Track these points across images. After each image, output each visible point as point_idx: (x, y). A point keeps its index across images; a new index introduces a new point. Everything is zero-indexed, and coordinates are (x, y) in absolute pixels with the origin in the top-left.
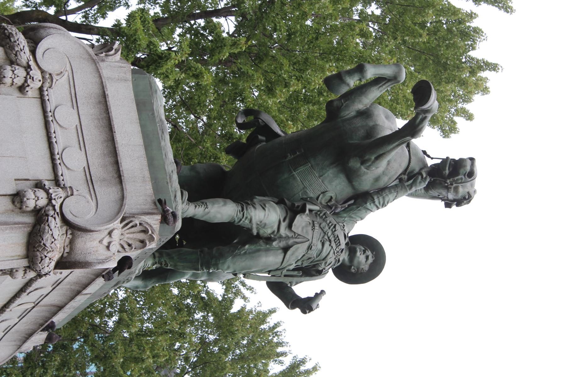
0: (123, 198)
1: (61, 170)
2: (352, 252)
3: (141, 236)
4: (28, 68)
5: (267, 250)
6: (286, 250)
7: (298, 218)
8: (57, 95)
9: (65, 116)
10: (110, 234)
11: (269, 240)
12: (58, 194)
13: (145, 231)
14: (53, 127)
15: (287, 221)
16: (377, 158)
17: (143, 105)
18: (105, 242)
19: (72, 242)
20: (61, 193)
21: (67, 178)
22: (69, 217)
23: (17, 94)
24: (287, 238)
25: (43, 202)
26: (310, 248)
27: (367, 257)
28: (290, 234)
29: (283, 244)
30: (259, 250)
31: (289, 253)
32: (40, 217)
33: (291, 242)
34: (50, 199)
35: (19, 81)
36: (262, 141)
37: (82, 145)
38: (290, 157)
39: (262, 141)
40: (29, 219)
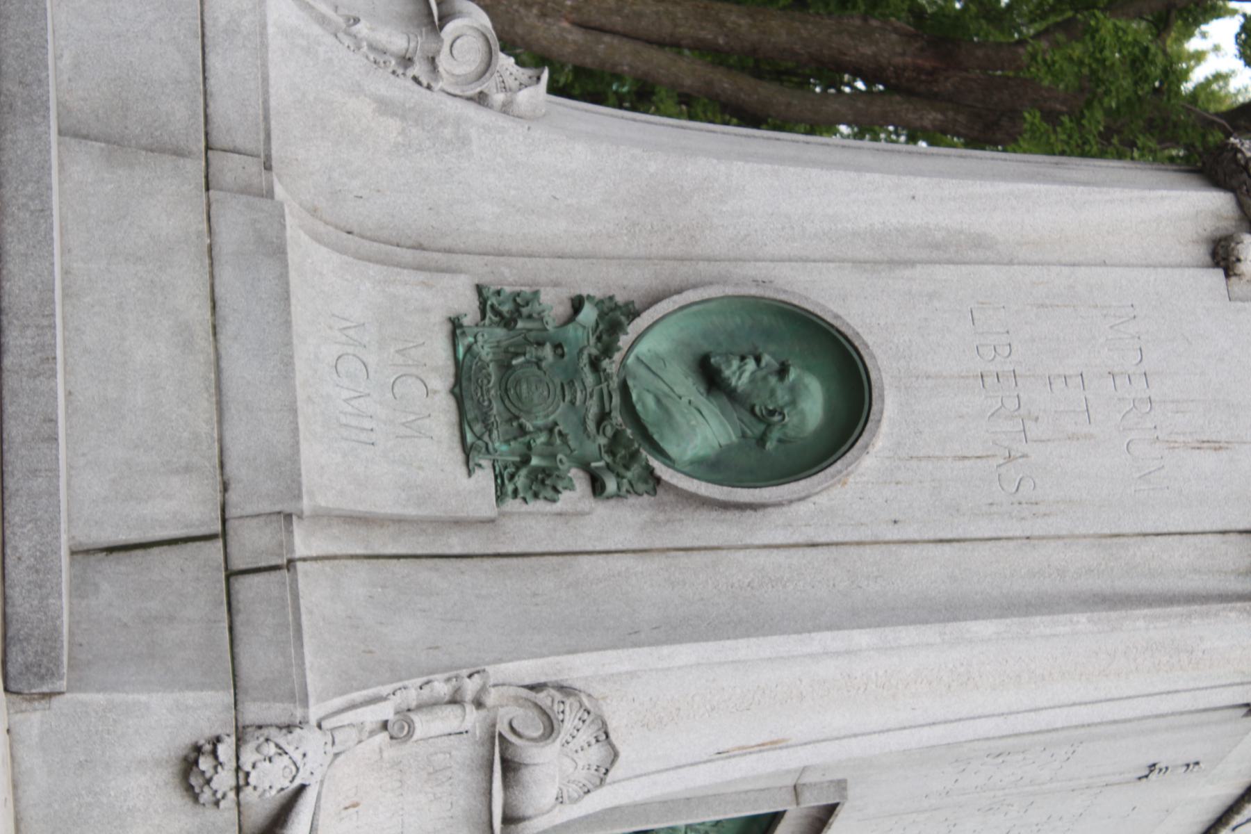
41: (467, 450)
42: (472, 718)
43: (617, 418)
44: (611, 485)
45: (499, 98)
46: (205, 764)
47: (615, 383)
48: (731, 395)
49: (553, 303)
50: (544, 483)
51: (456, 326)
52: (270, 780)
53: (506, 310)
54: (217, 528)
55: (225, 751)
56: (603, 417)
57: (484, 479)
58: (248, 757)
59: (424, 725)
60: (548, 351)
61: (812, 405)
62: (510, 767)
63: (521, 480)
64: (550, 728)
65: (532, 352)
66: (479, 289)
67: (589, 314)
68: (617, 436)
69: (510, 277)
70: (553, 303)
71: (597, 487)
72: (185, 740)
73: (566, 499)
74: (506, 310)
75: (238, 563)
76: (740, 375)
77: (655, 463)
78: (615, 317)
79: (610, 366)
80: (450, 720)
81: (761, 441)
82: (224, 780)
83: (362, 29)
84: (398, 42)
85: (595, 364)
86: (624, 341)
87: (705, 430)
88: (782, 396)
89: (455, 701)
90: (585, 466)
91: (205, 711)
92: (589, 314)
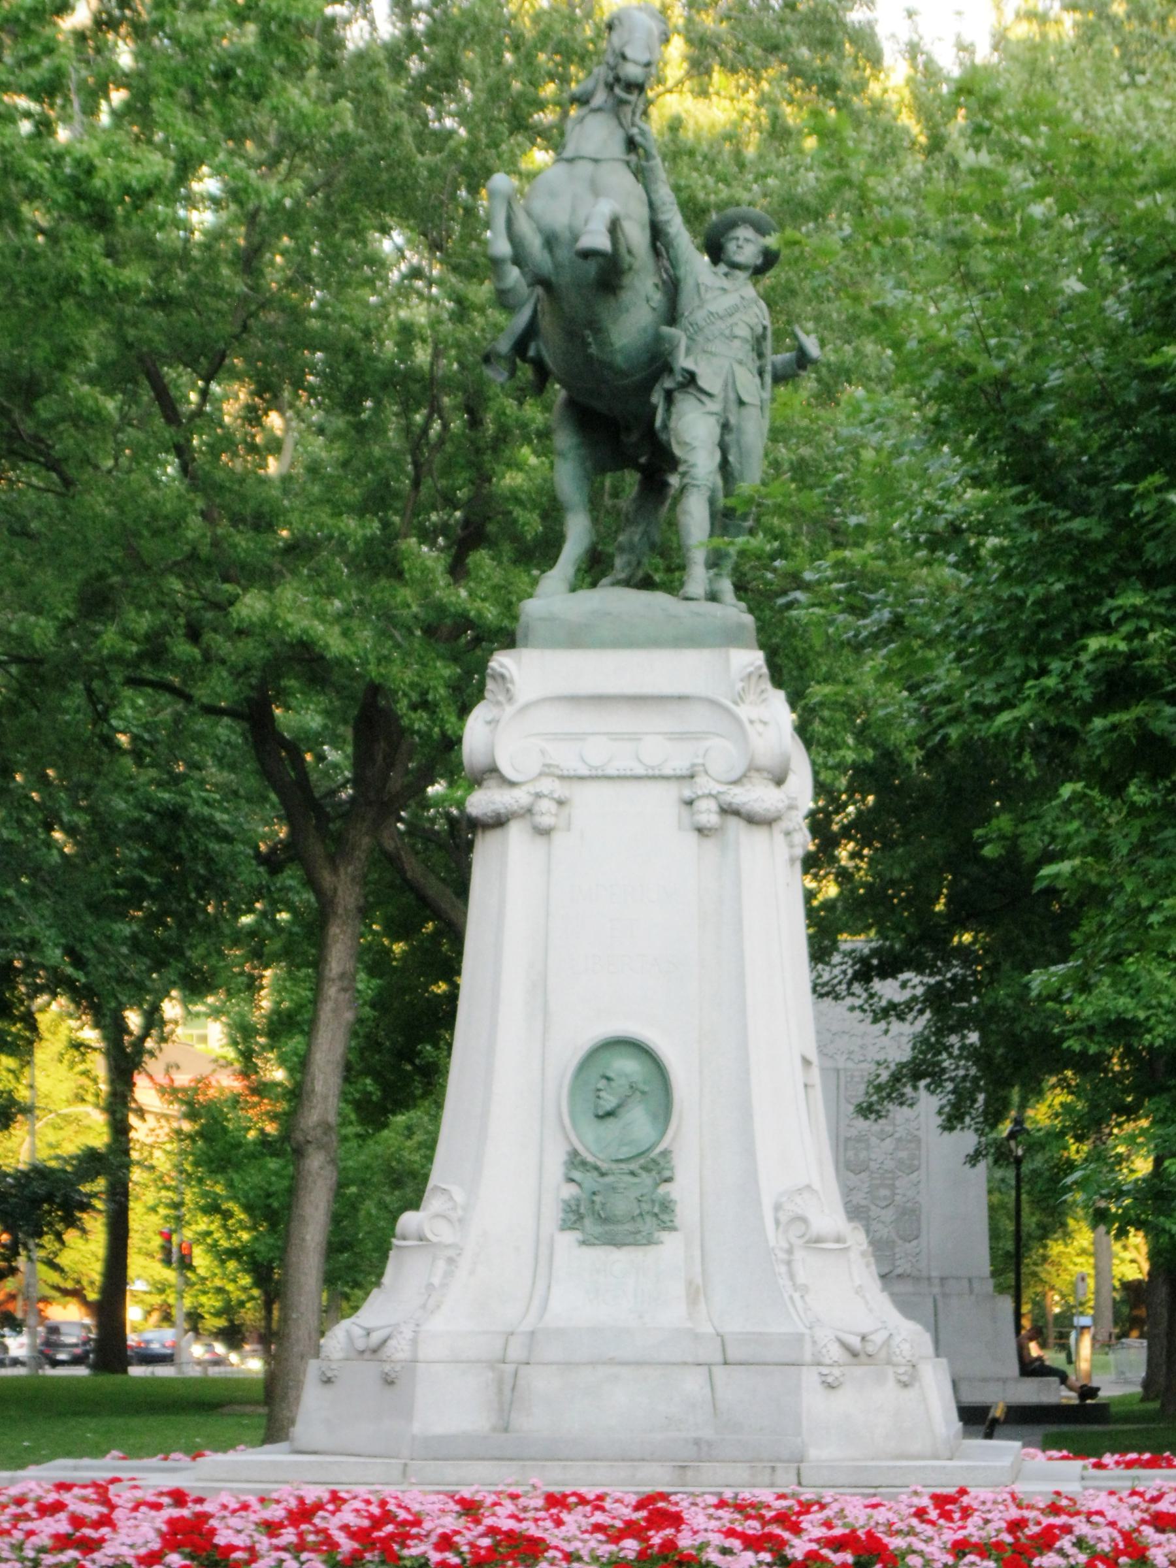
0: (713, 702)
1: (667, 771)
2: (735, 266)
3: (754, 679)
4: (539, 796)
5: (739, 429)
6: (741, 403)
7: (702, 383)
8: (567, 758)
9: (599, 753)
10: (751, 722)
11: (725, 427)
12: (704, 784)
13: (750, 675)
14: (611, 771)
15: (704, 398)
16: (630, 252)
17: (576, 637)
18: (760, 727)
19: (758, 770)
20: (701, 780)
21: (679, 765)
22: (735, 775)
23: (566, 810)
24: (726, 400)
25: (712, 805)
26: (740, 362)
27: (747, 240)
28: (720, 397)
29: (733, 406)
30: (738, 442)
31: (745, 398)
32: (728, 811)
33: (732, 396)
34: (710, 795)
35: (553, 807)
36: (538, 351)
37: (635, 737)
38: (593, 350)
39: (538, 351)
40: (733, 823)
41: (650, 1243)
42: (799, 1255)
43: (633, 1166)
44: (667, 1174)
45: (460, 1212)
46: (830, 1379)
47: (614, 1166)
48: (620, 1106)
49: (569, 1191)
50: (666, 1206)
51: (584, 1243)
52: (835, 1352)
53: (574, 1216)
54: (704, 1369)
55: (825, 1370)
56: (633, 1173)
57: (665, 1236)
58: (827, 1361)
59: (801, 1279)
60: (597, 1198)
61: (627, 1066)
62: (818, 1240)
63: (665, 1217)
64: (803, 1220)
65: (598, 1207)
66: (562, 1229)
67: (577, 1175)
68: (643, 1168)
69: (552, 1214)
70: (569, 1191)
71: (668, 1180)
72: (820, 1388)
73: (675, 1196)
74: (574, 1216)
75: (719, 1358)
76: (609, 1101)
77: (658, 1150)
78: (575, 1161)
79: (604, 1167)
80: (798, 1267)
81: (643, 1093)
82: (836, 1372)
83: (436, 1281)
84: (441, 1264)
85: (603, 1174)
86: (590, 1159)
87: (638, 1120)
88: (623, 1081)
89: (789, 1263)
90: (657, 1185)
91: (810, 1378)
92: (577, 1175)
